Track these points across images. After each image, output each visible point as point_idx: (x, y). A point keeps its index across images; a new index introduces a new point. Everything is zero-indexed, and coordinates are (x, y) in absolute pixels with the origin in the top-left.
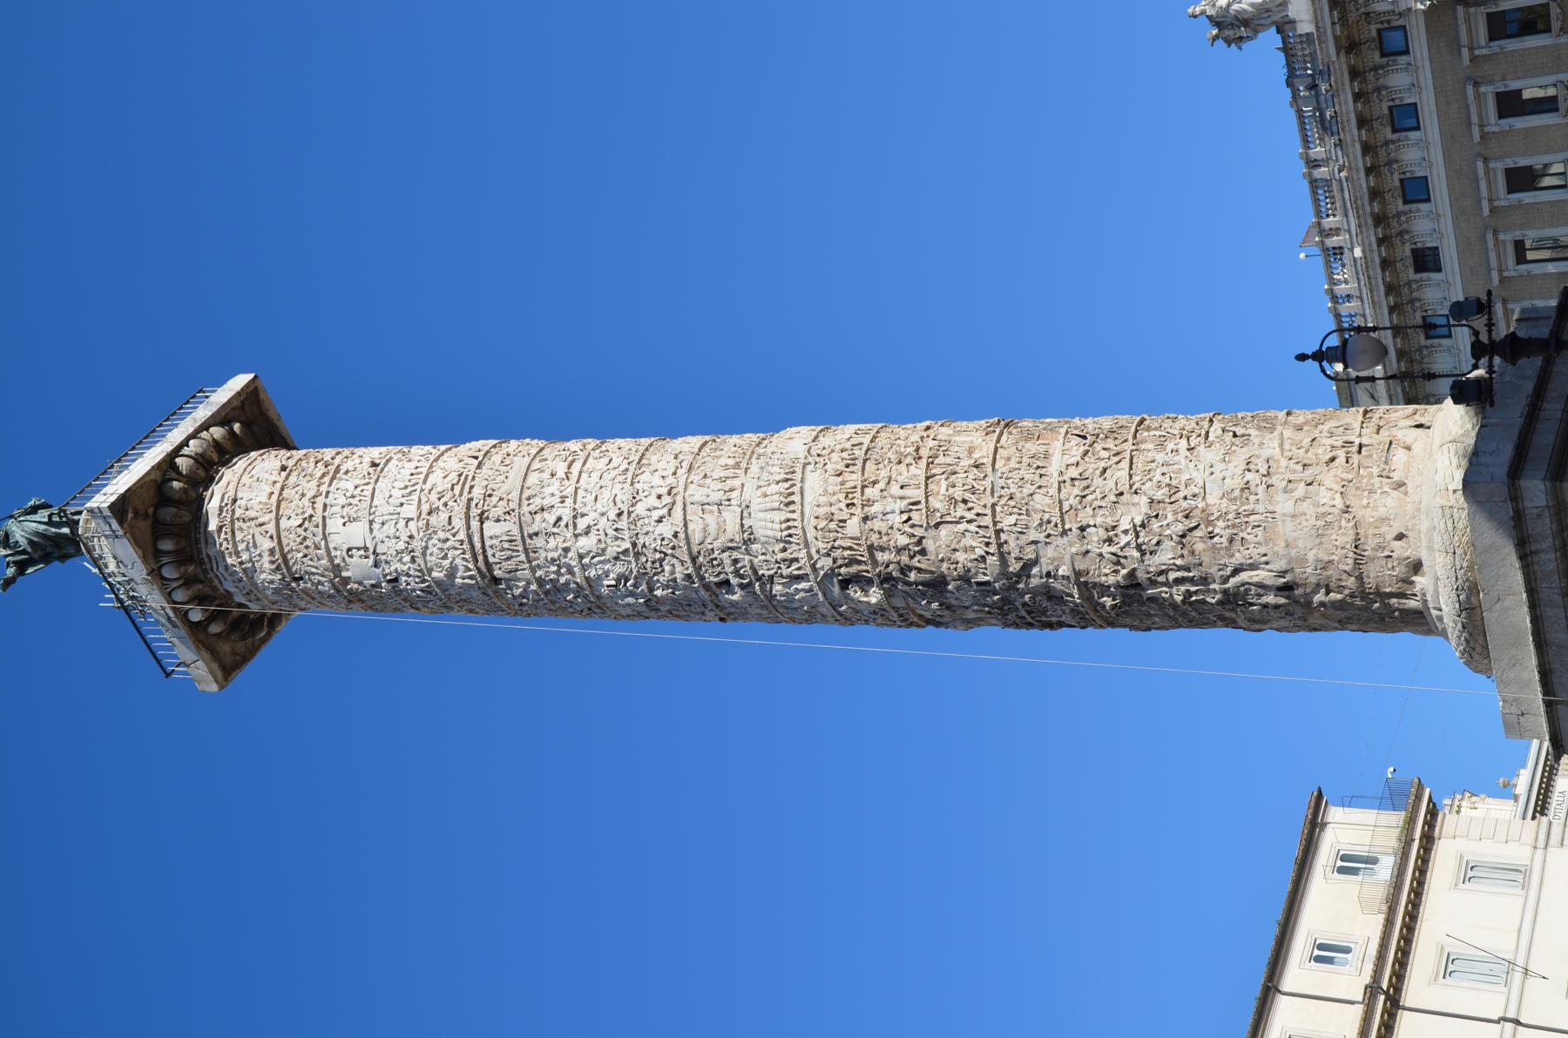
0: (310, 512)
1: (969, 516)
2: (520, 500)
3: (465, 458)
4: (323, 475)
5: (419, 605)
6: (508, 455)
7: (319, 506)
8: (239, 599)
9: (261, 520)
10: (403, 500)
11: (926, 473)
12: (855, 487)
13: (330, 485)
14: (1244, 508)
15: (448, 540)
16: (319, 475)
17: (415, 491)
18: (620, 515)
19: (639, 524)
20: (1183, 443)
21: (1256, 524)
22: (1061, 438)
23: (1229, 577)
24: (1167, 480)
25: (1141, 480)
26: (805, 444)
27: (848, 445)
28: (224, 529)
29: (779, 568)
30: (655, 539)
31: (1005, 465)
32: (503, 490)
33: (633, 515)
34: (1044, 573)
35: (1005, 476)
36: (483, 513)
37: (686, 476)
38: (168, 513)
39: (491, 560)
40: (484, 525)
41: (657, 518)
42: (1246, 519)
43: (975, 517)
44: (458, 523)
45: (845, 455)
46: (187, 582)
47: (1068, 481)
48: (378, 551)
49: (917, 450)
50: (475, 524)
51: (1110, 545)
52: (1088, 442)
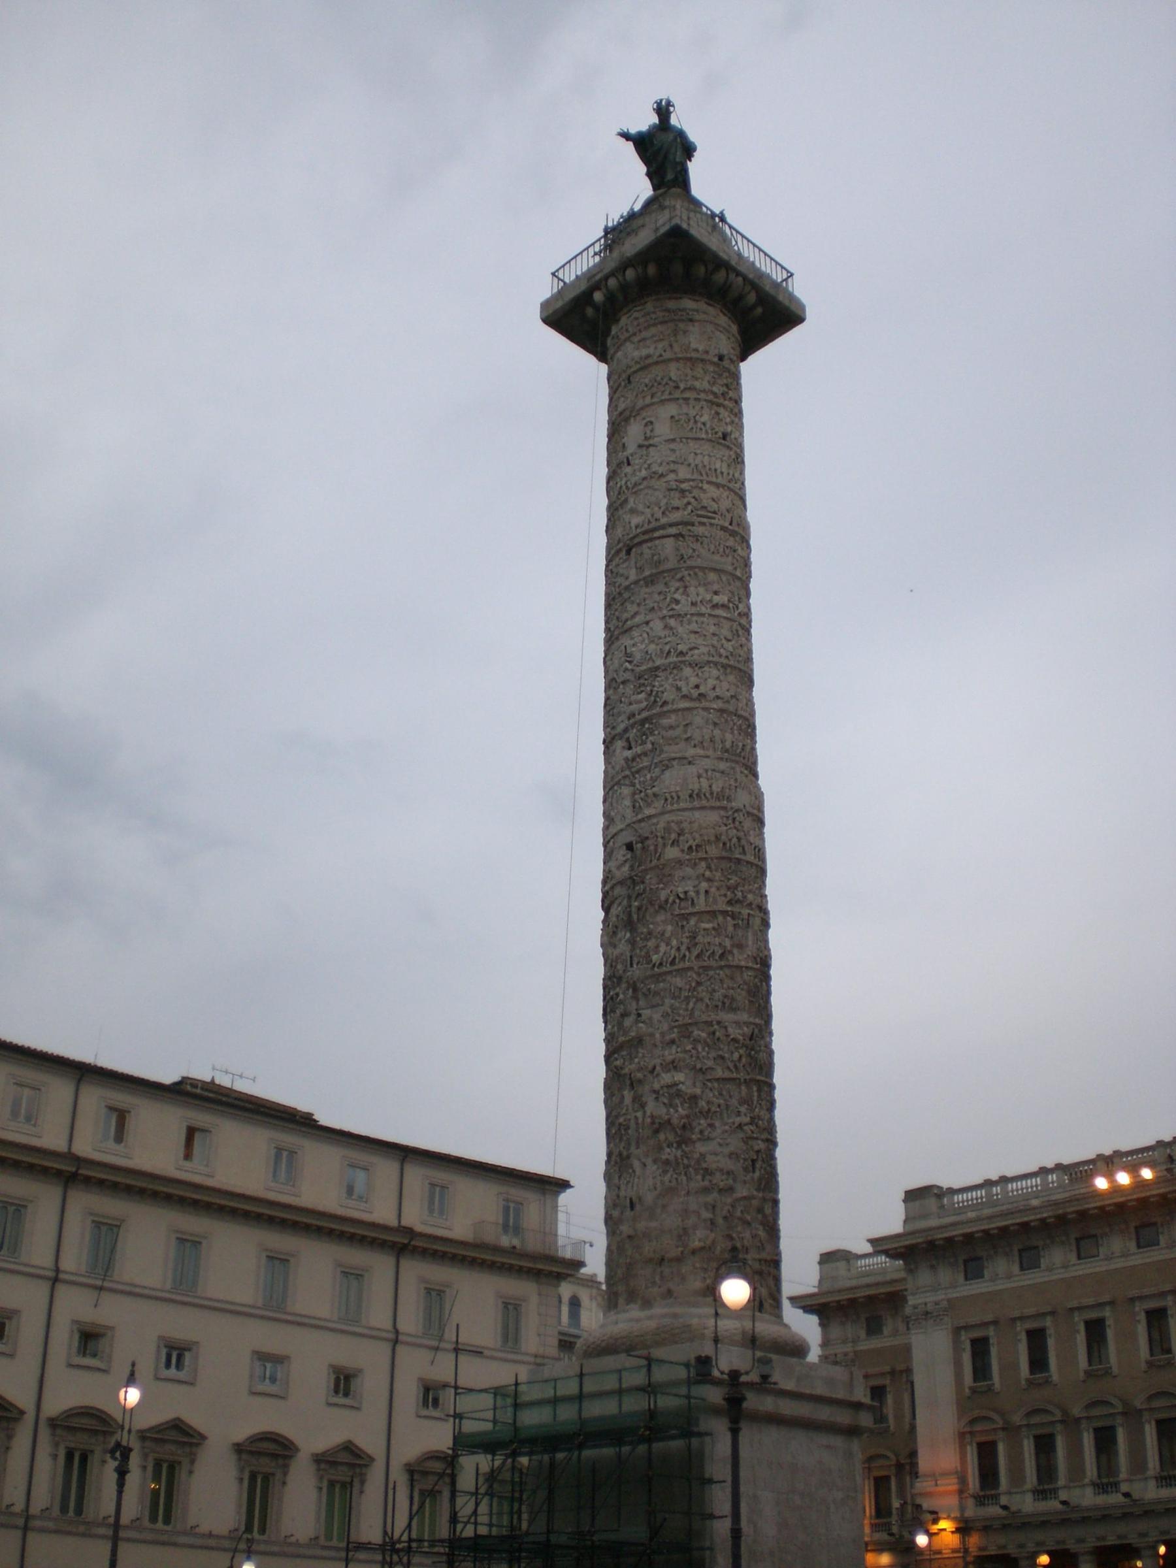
0: (682, 386)
1: (683, 948)
2: (696, 567)
3: (731, 515)
4: (715, 394)
5: (611, 484)
6: (735, 551)
7: (687, 395)
8: (614, 330)
9: (676, 346)
10: (693, 465)
11: (719, 911)
12: (706, 852)
13: (706, 400)
15: (660, 508)
16: (715, 389)
17: (701, 475)
18: (681, 653)
19: (675, 671)
20: (748, 1120)
21: (679, 1181)
22: (751, 1020)
23: (640, 1160)
24: (713, 1109)
26: (744, 806)
27: (743, 842)
28: (667, 314)
29: (641, 792)
30: (662, 686)
31: (726, 975)
32: (702, 550)
33: (682, 666)
34: (640, 1012)
35: (717, 976)
36: (683, 536)
37: (715, 706)
38: (678, 268)
39: (645, 546)
40: (672, 538)
41: (679, 685)
43: (682, 955)
44: (675, 516)
45: (735, 840)
46: (624, 287)
47: (712, 1029)
48: (651, 449)
49: (738, 901)
50: (673, 530)
51: (661, 1064)
52: (748, 1042)
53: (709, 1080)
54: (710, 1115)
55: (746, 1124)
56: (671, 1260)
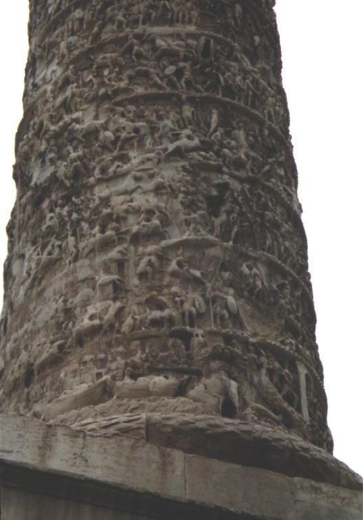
14: (85, 225)
25: (130, 112)
42: (70, 233)
53: (120, 104)
54: (119, 143)
55: (195, 149)
56: (43, 366)
